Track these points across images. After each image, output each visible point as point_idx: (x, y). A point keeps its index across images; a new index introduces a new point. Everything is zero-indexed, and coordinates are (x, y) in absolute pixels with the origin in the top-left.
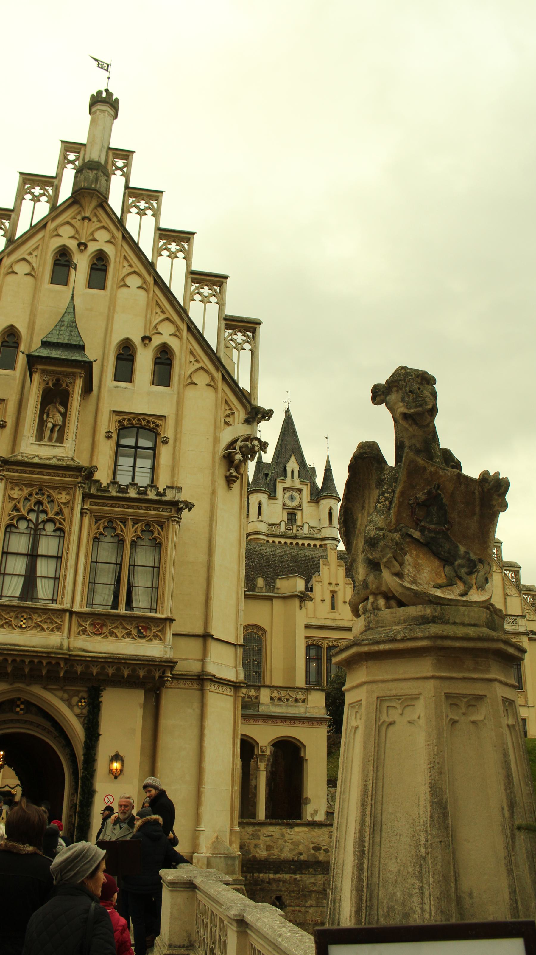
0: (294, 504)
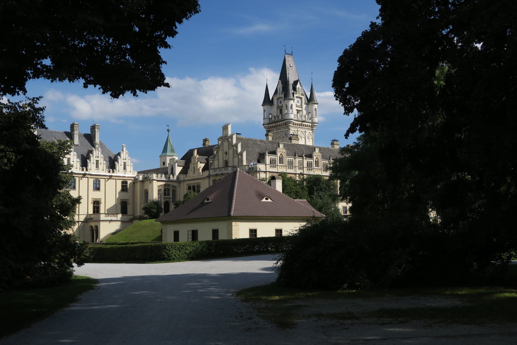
0: (281, 105)
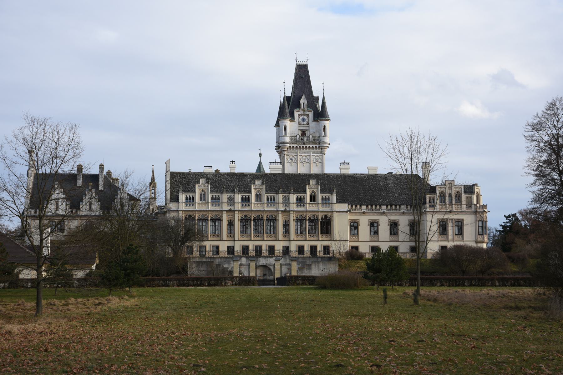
0: (305, 123)
